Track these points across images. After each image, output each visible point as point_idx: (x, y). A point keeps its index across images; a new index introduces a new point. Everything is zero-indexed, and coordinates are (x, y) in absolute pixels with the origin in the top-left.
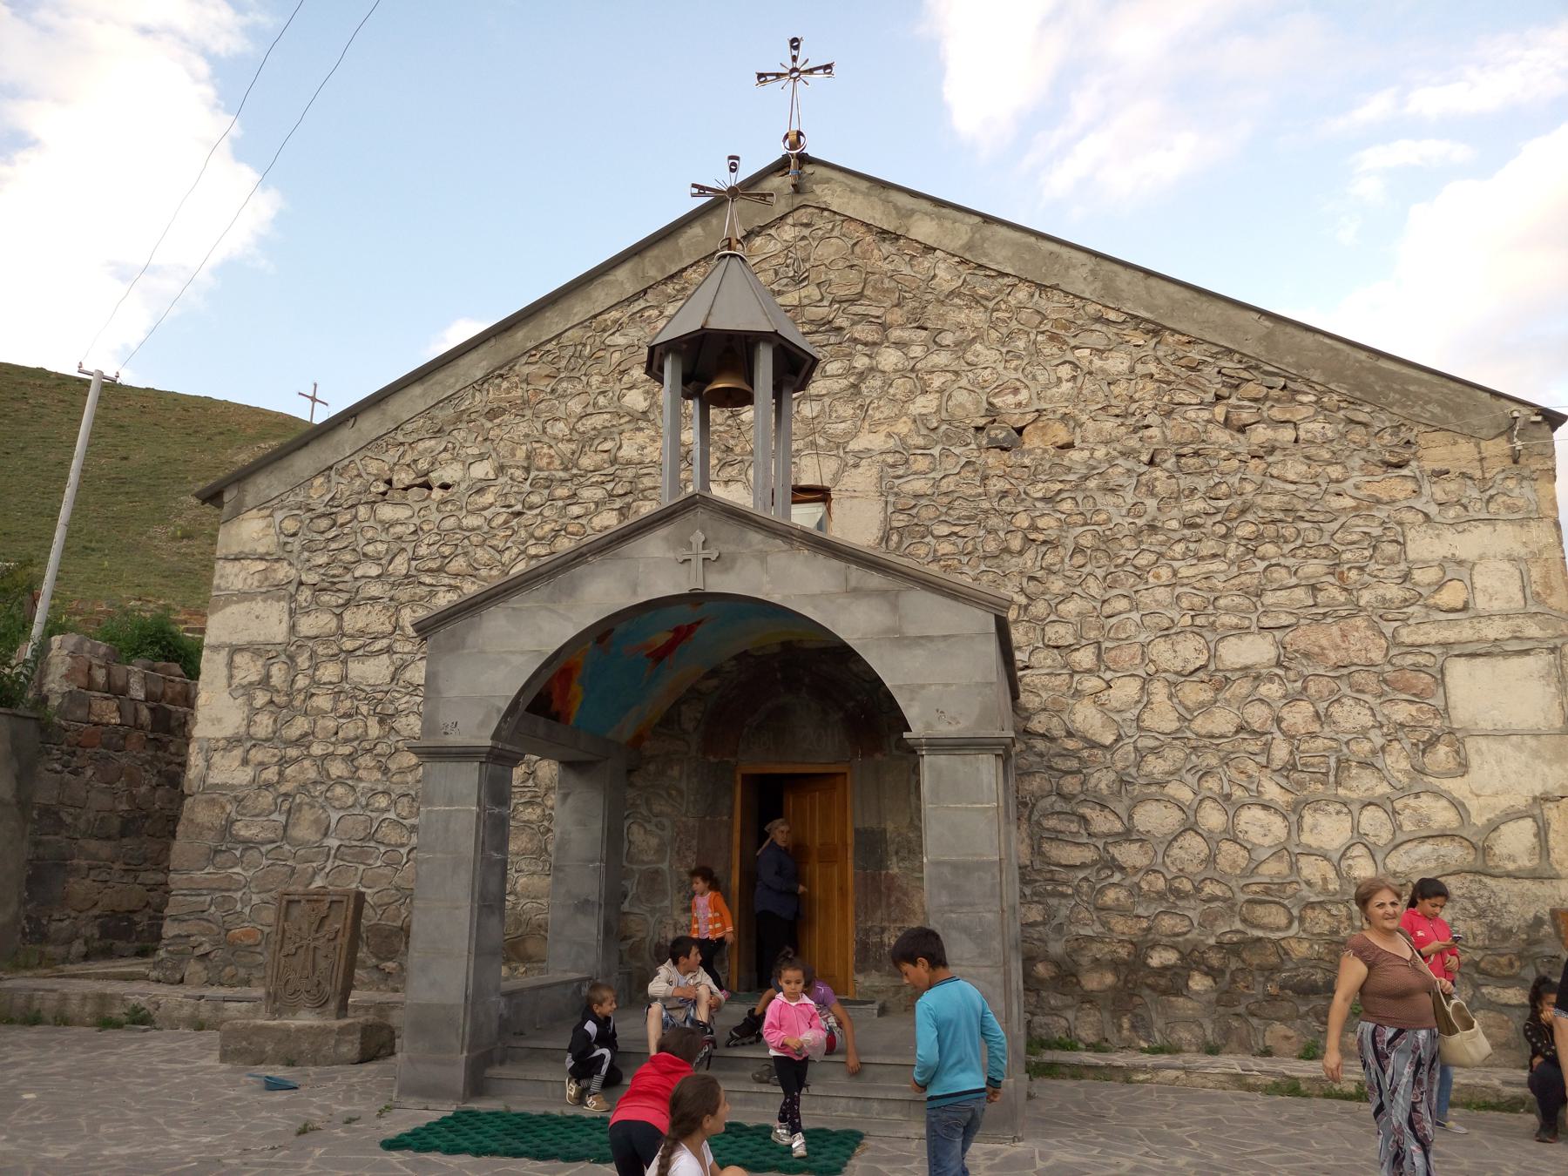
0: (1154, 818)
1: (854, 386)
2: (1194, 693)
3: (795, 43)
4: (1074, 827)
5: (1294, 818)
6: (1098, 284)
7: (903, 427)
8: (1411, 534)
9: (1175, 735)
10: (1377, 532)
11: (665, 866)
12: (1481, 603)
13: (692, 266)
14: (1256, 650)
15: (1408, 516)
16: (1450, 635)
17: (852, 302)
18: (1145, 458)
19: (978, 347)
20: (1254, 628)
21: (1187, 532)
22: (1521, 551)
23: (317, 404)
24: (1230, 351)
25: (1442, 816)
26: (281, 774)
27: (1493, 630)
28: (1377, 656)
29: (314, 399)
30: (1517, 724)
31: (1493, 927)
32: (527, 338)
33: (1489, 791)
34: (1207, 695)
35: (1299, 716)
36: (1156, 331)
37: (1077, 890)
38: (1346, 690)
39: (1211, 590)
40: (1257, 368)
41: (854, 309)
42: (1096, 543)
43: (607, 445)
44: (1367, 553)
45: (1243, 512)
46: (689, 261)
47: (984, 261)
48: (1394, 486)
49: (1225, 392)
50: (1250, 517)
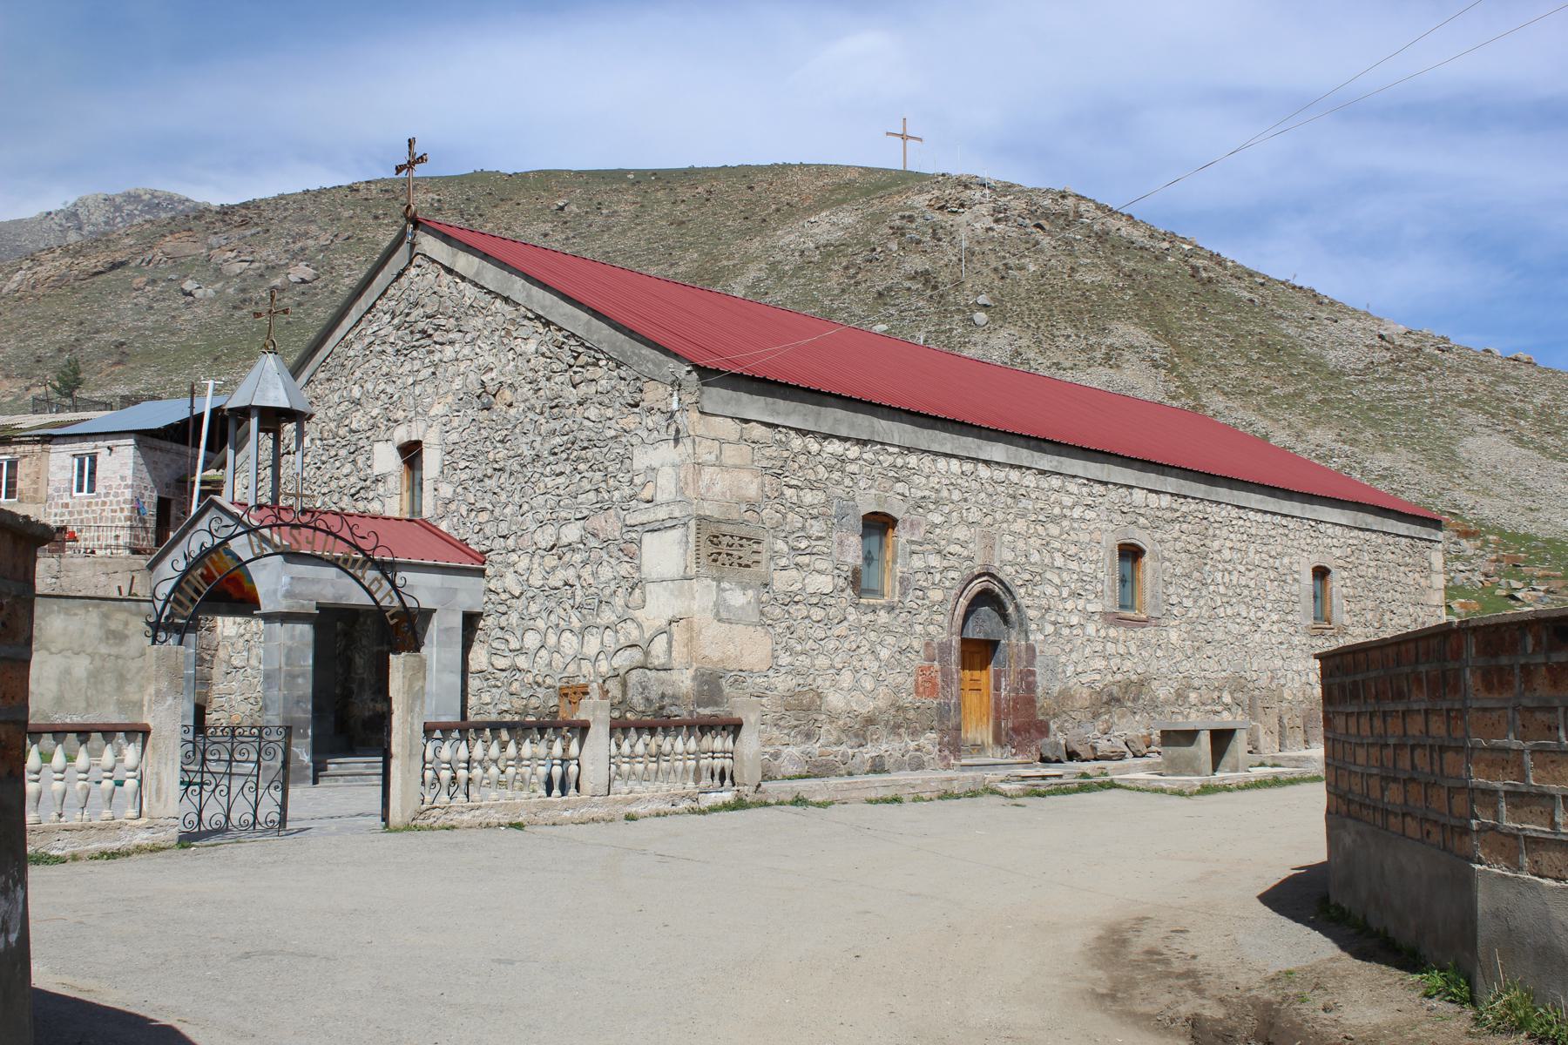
0: (532, 640)
1: (434, 373)
2: (551, 561)
3: (411, 142)
4: (503, 647)
5: (580, 637)
6: (525, 293)
7: (450, 399)
8: (635, 452)
9: (541, 588)
10: (622, 452)
11: (365, 676)
12: (659, 498)
13: (379, 298)
14: (572, 533)
15: (634, 440)
16: (644, 519)
17: (433, 316)
18: (537, 411)
19: (479, 342)
20: (572, 520)
21: (552, 458)
22: (678, 460)
23: (909, 142)
24: (574, 335)
25: (635, 634)
26: (245, 629)
27: (662, 513)
28: (617, 534)
29: (904, 137)
30: (666, 576)
31: (647, 699)
32: (321, 356)
33: (652, 617)
34: (555, 563)
35: (586, 573)
36: (547, 324)
37: (503, 683)
38: (606, 557)
39: (558, 495)
40: (583, 344)
41: (436, 321)
42: (519, 468)
43: (346, 423)
44: (618, 466)
45: (573, 443)
46: (376, 297)
47: (482, 283)
48: (630, 421)
49: (572, 361)
50: (576, 446)
